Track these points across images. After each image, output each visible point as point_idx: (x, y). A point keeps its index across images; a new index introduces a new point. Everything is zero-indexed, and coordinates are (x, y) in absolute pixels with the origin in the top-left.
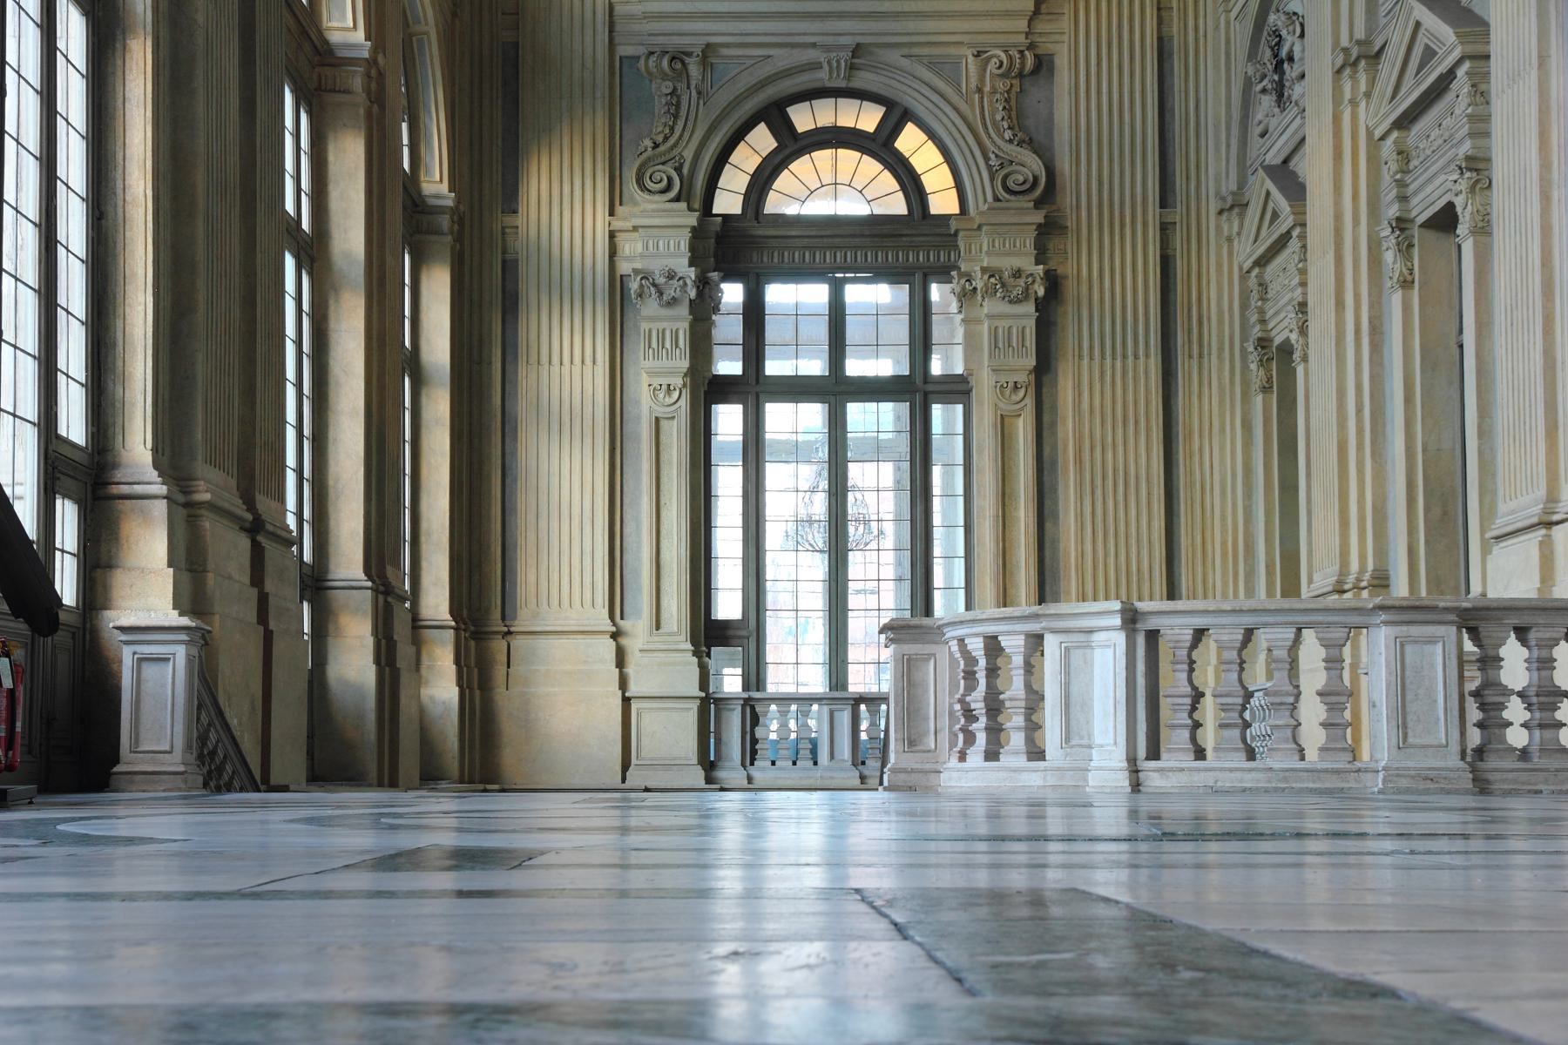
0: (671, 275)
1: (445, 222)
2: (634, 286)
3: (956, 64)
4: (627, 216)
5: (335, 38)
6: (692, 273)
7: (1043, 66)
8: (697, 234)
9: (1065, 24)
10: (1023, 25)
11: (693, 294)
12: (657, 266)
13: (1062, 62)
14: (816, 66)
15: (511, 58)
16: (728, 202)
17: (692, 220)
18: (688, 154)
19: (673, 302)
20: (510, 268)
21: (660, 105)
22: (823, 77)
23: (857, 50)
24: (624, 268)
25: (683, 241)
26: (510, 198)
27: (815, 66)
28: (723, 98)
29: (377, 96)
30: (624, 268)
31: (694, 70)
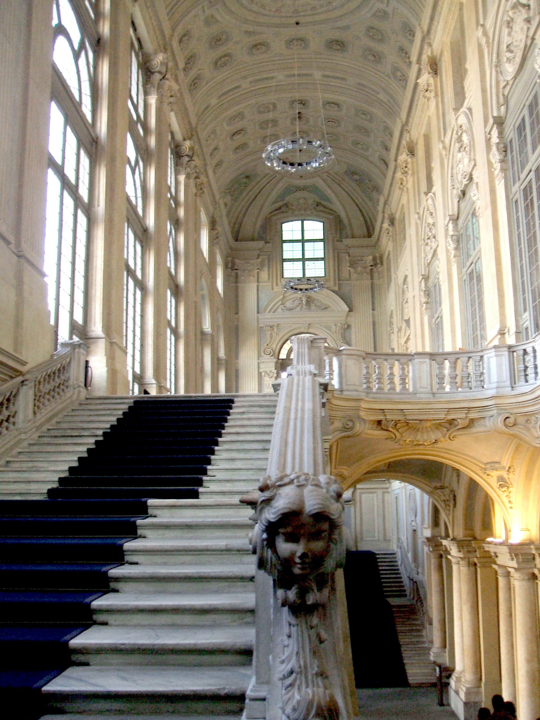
0: (271, 372)
1: (224, 362)
2: (263, 374)
3: (330, 327)
4: (262, 360)
5: (205, 330)
6: (275, 371)
7: (349, 327)
8: (276, 363)
9: (353, 318)
10: (344, 318)
11: (275, 375)
12: (268, 370)
13: (353, 326)
14: (300, 328)
15: (237, 328)
16: (283, 355)
17: (275, 360)
18: (274, 346)
19: (271, 377)
20: (237, 371)
21: (268, 336)
22: (303, 330)
23: (309, 325)
24: (261, 370)
25: (273, 365)
26: (237, 357)
27: (300, 328)
28: (281, 335)
29: (213, 340)
30: (261, 370)
31: (275, 329)
